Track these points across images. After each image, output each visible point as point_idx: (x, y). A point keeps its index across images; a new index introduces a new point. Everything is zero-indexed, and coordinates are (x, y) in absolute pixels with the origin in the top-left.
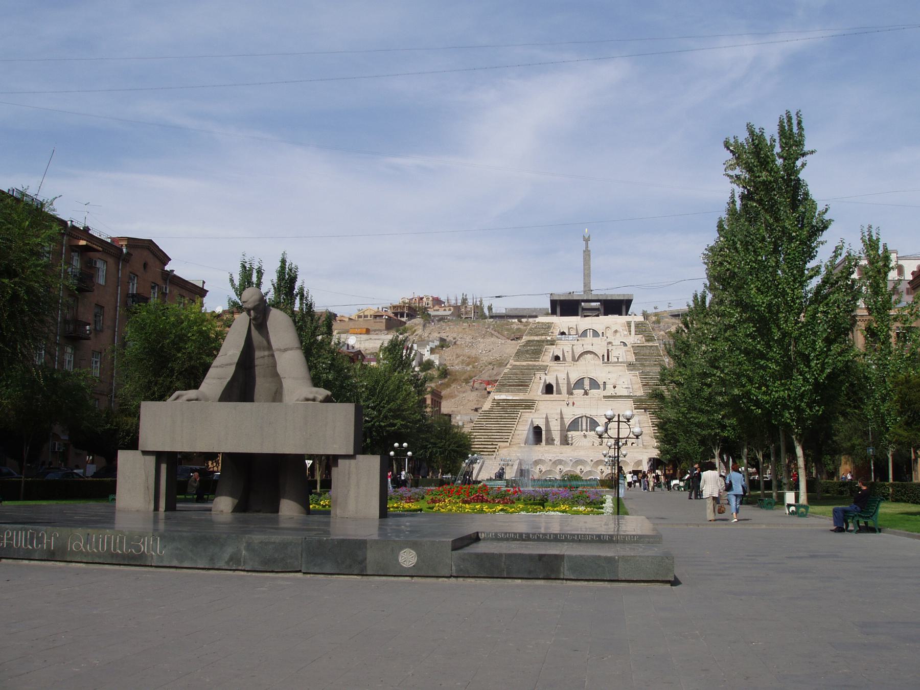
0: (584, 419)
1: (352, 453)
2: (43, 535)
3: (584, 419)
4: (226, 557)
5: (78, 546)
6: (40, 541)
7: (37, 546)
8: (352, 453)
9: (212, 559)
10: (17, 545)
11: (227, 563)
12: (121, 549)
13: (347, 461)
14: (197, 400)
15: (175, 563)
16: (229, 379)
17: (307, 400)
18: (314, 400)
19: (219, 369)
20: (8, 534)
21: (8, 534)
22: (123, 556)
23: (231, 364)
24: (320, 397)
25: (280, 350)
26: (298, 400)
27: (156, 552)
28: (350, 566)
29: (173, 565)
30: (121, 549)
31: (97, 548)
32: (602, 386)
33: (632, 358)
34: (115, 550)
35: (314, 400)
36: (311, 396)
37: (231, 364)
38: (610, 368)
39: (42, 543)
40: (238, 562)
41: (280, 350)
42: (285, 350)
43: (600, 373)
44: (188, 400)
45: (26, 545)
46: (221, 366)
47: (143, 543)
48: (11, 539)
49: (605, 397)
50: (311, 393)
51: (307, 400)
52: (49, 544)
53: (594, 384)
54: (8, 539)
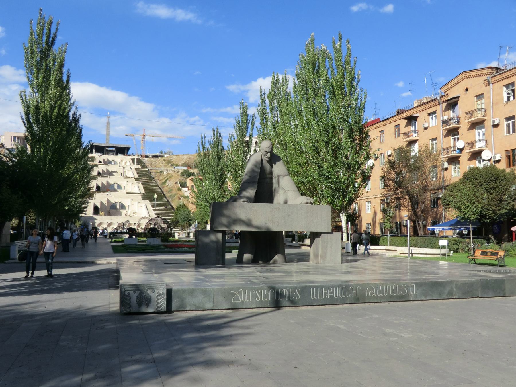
0: (118, 203)
1: (330, 231)
2: (352, 288)
3: (118, 203)
4: (446, 292)
5: (372, 293)
6: (350, 292)
7: (348, 295)
8: (330, 231)
9: (440, 294)
10: (336, 296)
11: (447, 295)
12: (396, 293)
13: (326, 235)
15: (423, 298)
17: (307, 203)
20: (330, 290)
21: (330, 290)
22: (397, 296)
27: (413, 293)
28: (499, 292)
29: (422, 299)
30: (396, 293)
31: (383, 293)
32: (123, 188)
33: (137, 176)
34: (392, 293)
36: (309, 201)
38: (127, 179)
39: (351, 293)
40: (452, 295)
42: (284, 176)
43: (123, 182)
45: (341, 296)
47: (407, 289)
48: (333, 293)
49: (127, 193)
51: (307, 203)
52: (355, 294)
53: (119, 187)
54: (330, 293)
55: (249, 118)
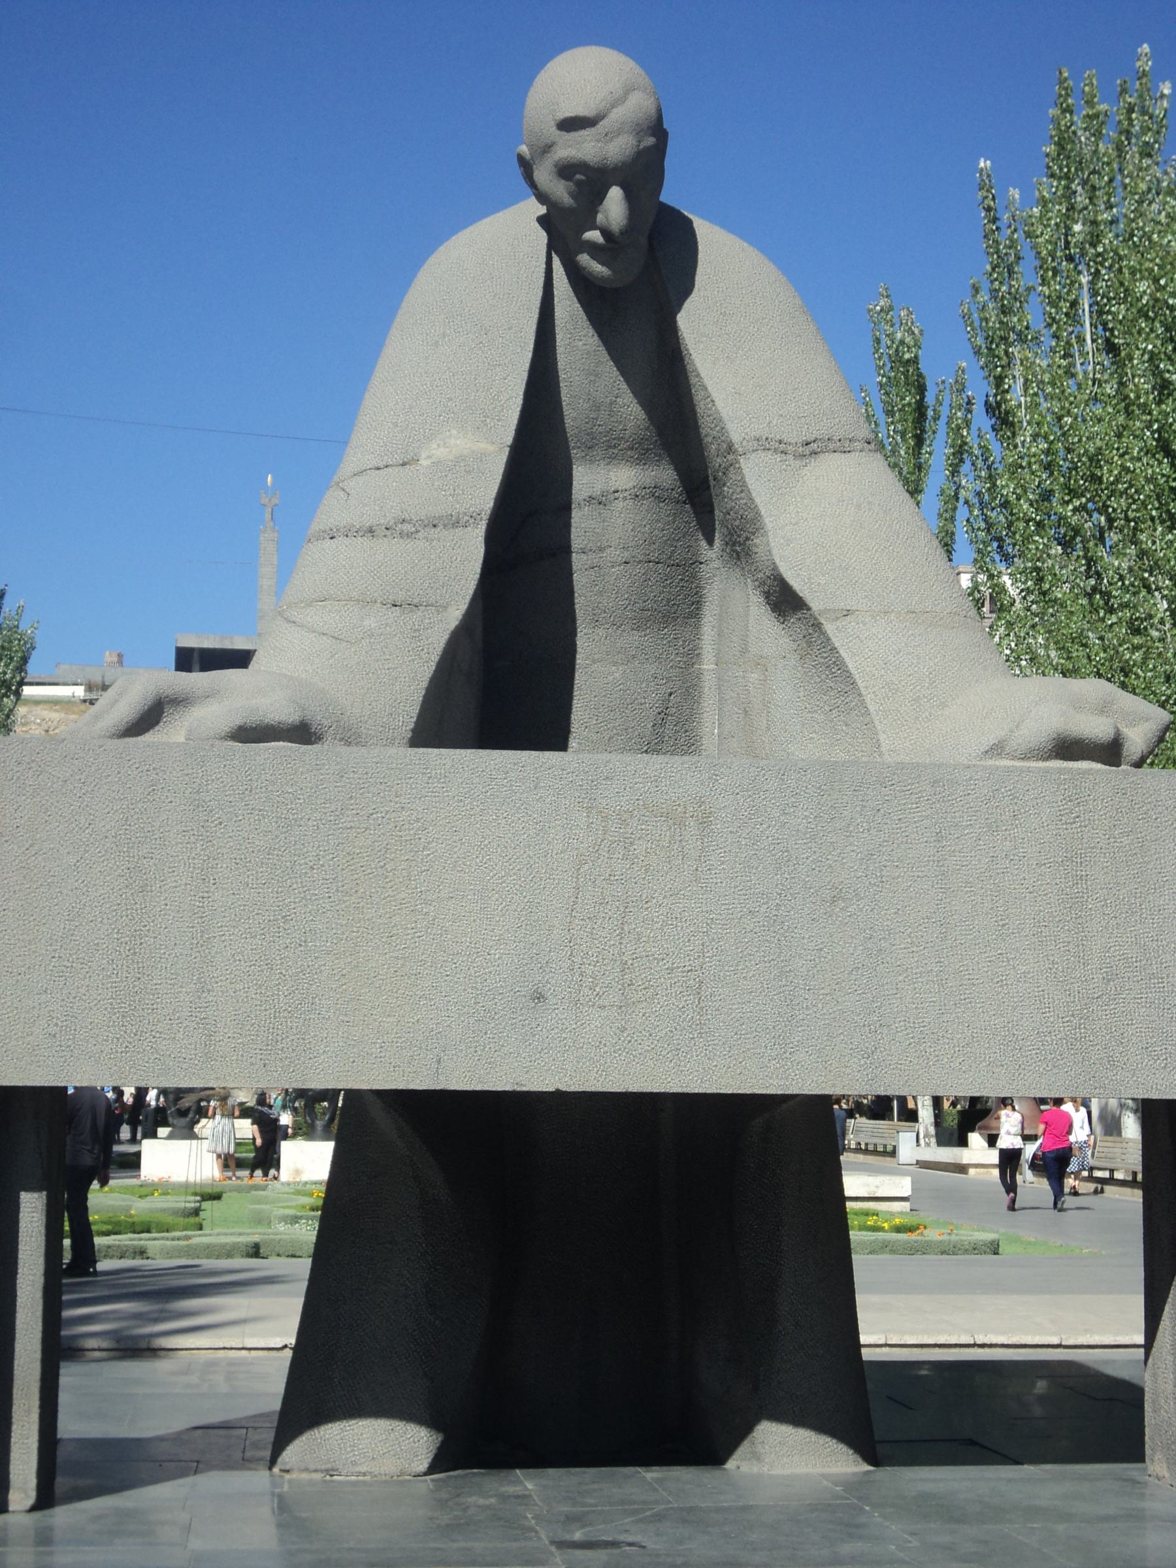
14: (302, 733)
16: (455, 614)
17: (1068, 748)
18: (1110, 752)
19: (386, 549)
23: (455, 523)
24: (1137, 739)
25: (780, 447)
26: (997, 749)
35: (1110, 752)
36: (1097, 728)
37: (455, 523)
41: (764, 444)
42: (811, 449)
44: (251, 734)
46: (401, 528)
50: (1078, 705)
51: (1068, 748)
55: (930, 399)
